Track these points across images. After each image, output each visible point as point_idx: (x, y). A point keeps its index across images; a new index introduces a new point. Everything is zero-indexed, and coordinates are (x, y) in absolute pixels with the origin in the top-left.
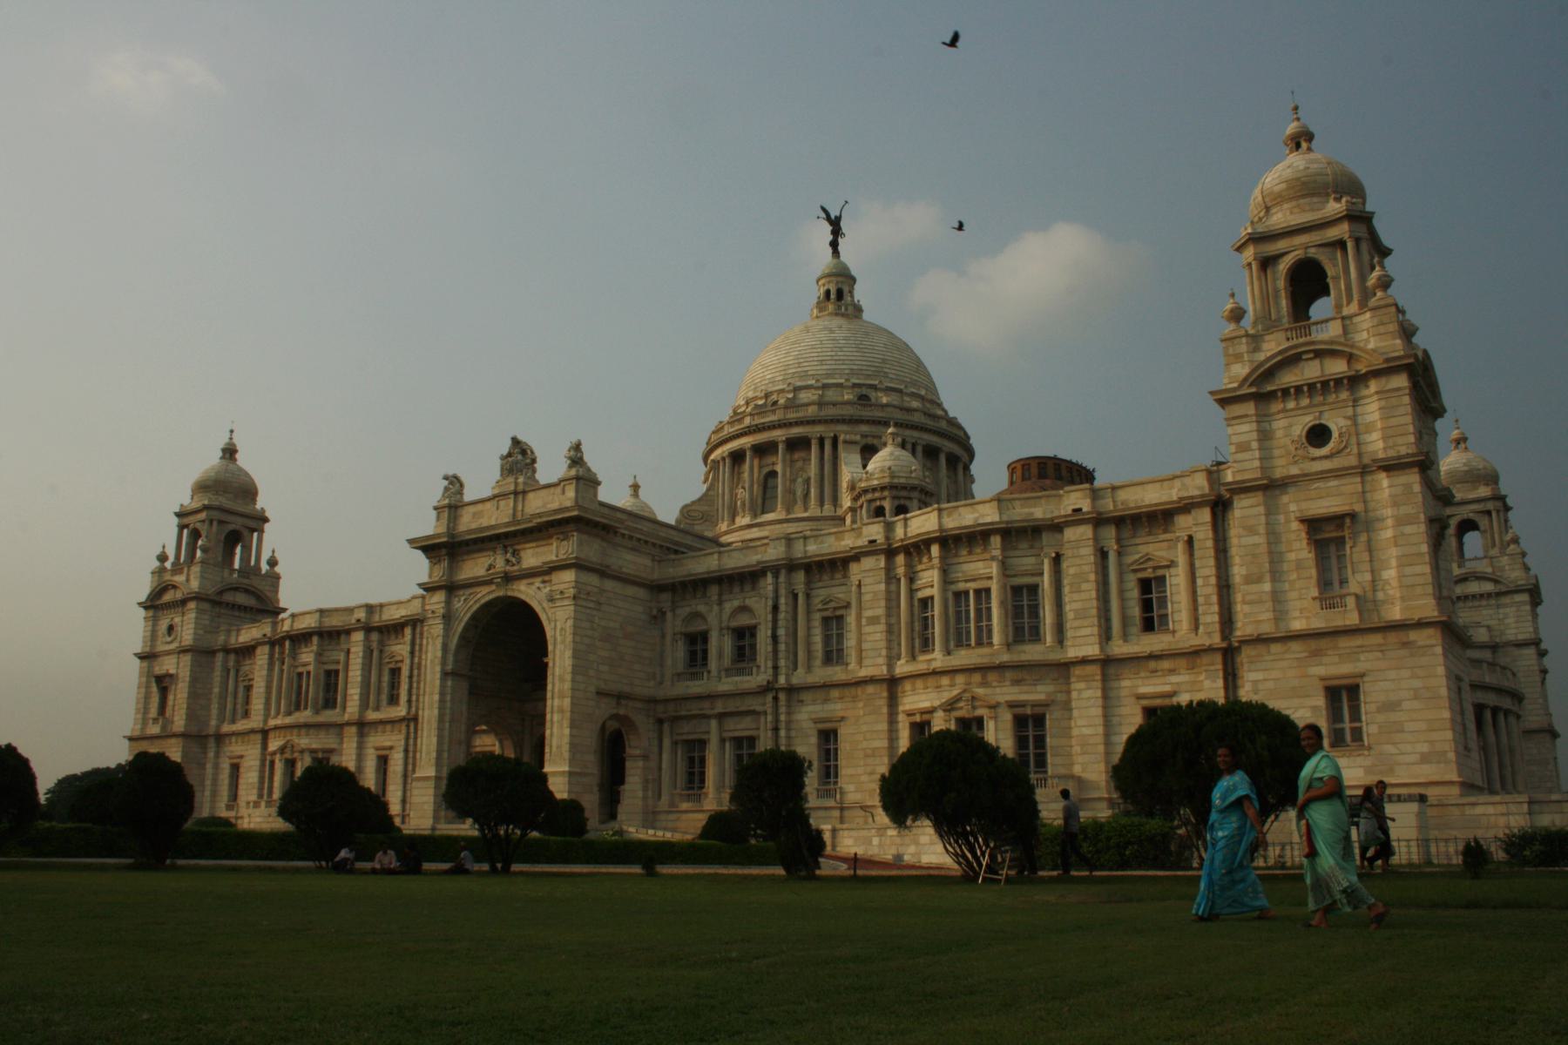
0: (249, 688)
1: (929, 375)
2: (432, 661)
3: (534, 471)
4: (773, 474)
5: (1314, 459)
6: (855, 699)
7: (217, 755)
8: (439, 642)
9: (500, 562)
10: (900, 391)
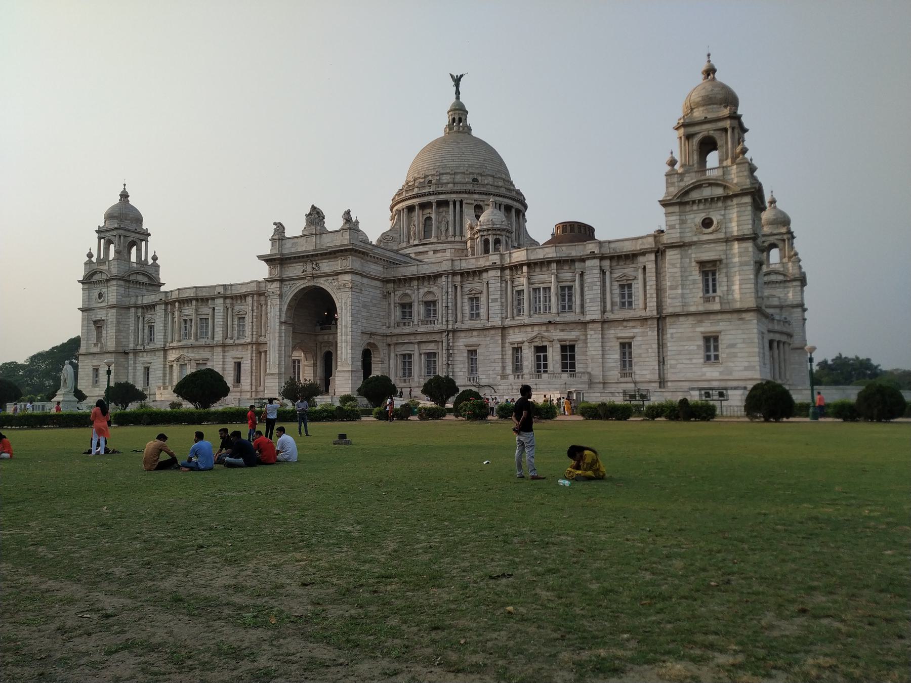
0: (151, 328)
1: (506, 168)
3: (324, 223)
4: (429, 218)
5: (705, 234)
6: (485, 336)
7: (135, 363)
9: (309, 269)
10: (493, 176)
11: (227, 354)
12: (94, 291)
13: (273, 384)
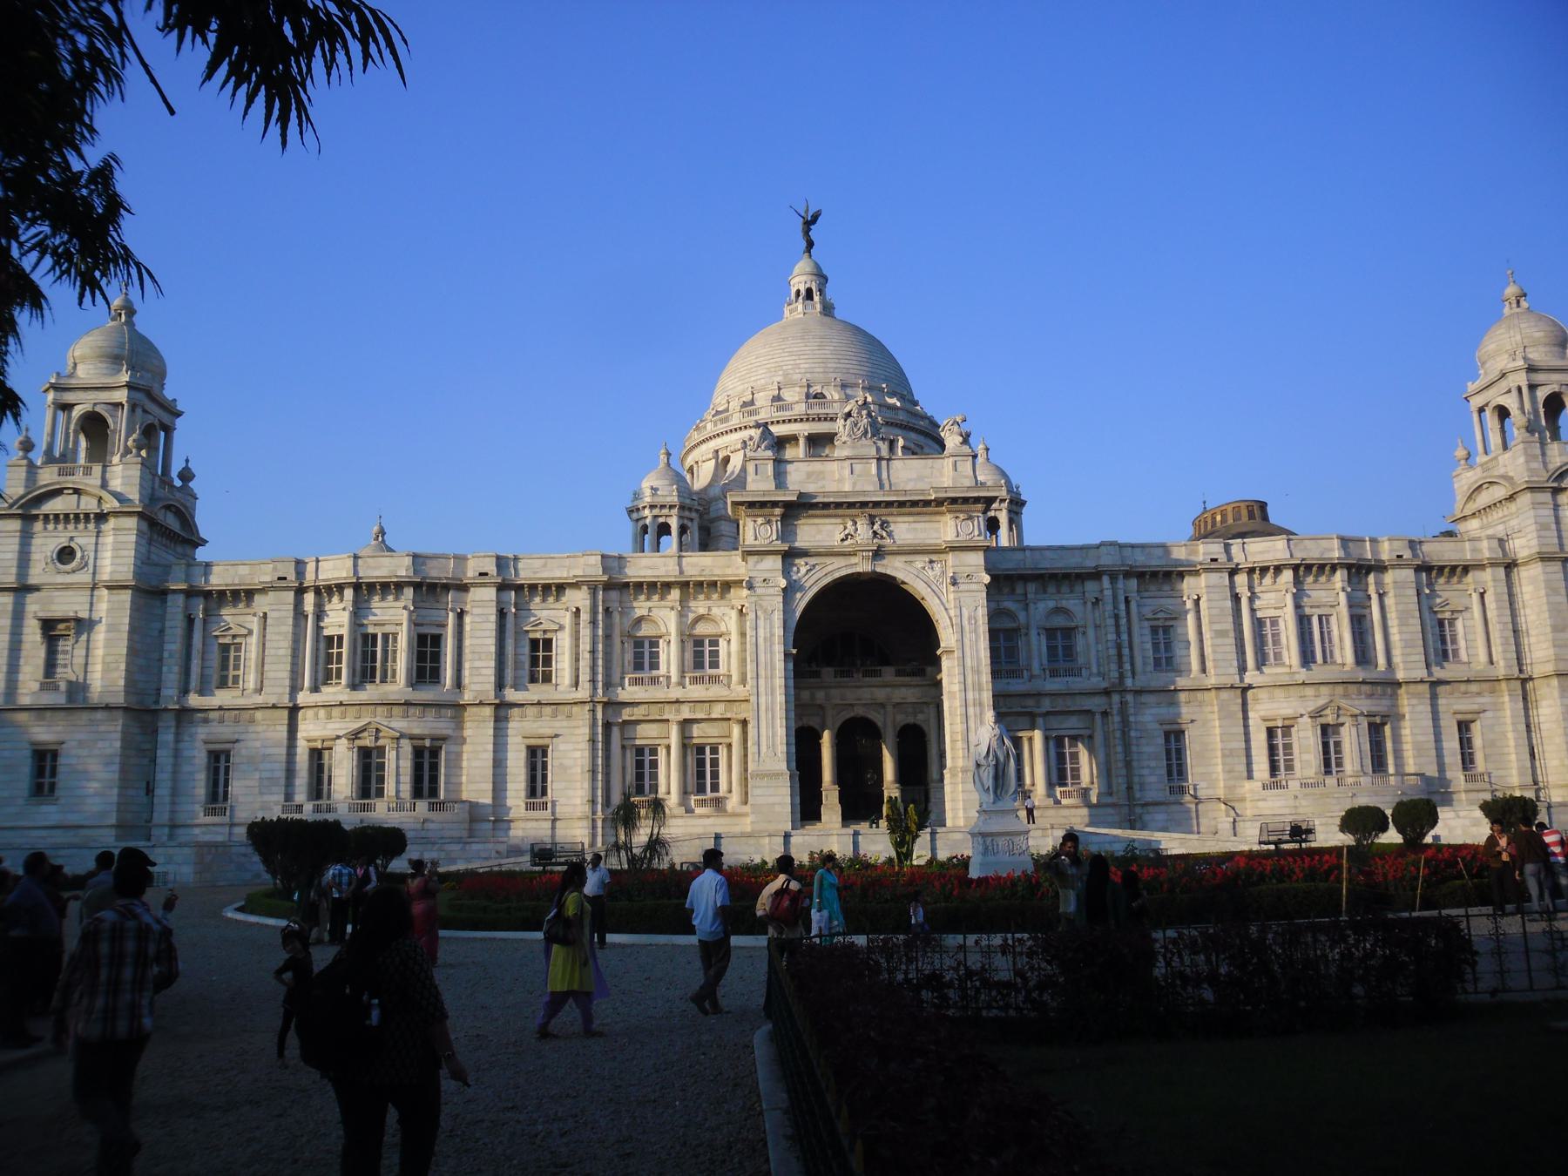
2: (765, 639)
8: (778, 618)
11: (502, 725)
13: (771, 800)
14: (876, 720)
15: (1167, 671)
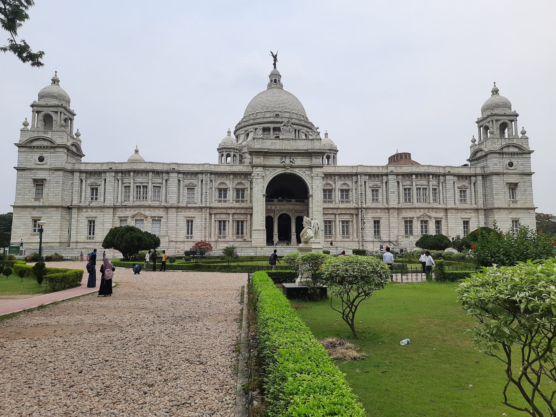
2: (258, 191)
9: (288, 161)
12: (33, 154)
14: (289, 215)
15: (376, 203)
